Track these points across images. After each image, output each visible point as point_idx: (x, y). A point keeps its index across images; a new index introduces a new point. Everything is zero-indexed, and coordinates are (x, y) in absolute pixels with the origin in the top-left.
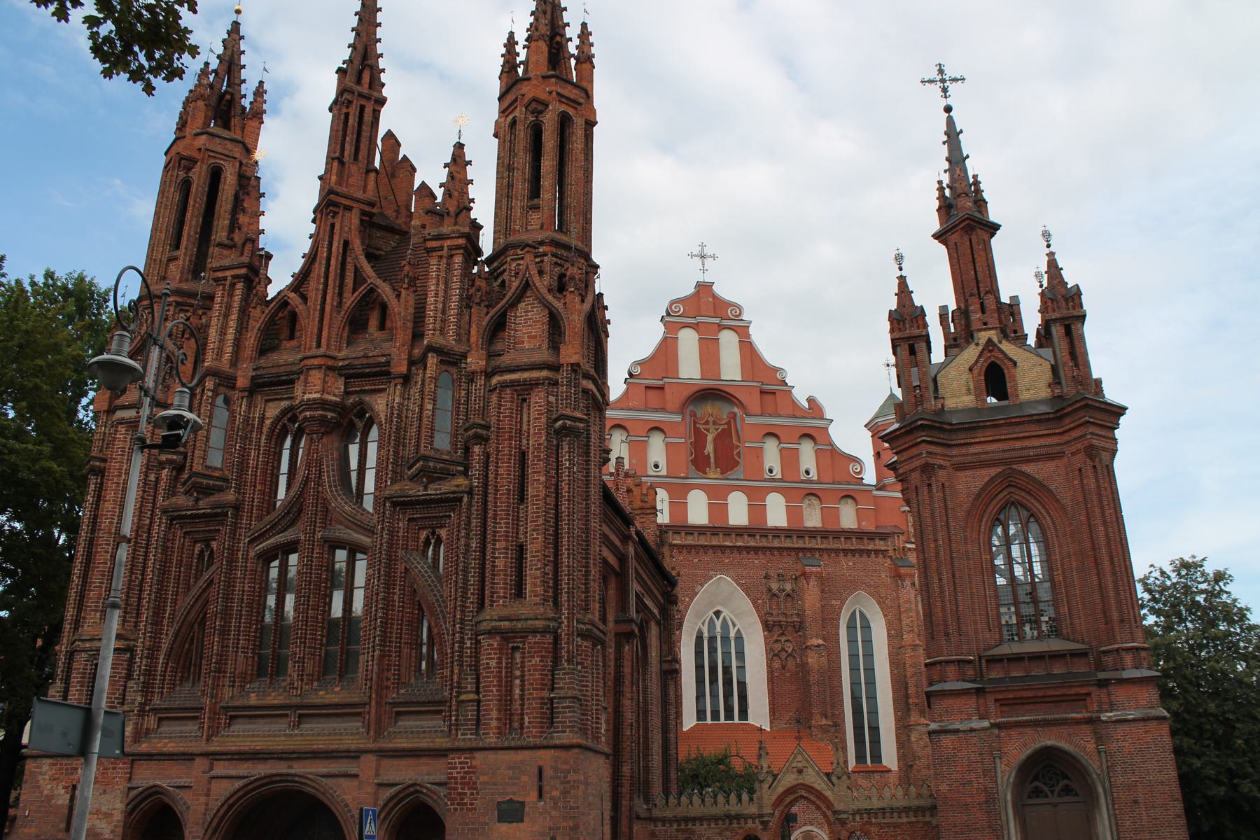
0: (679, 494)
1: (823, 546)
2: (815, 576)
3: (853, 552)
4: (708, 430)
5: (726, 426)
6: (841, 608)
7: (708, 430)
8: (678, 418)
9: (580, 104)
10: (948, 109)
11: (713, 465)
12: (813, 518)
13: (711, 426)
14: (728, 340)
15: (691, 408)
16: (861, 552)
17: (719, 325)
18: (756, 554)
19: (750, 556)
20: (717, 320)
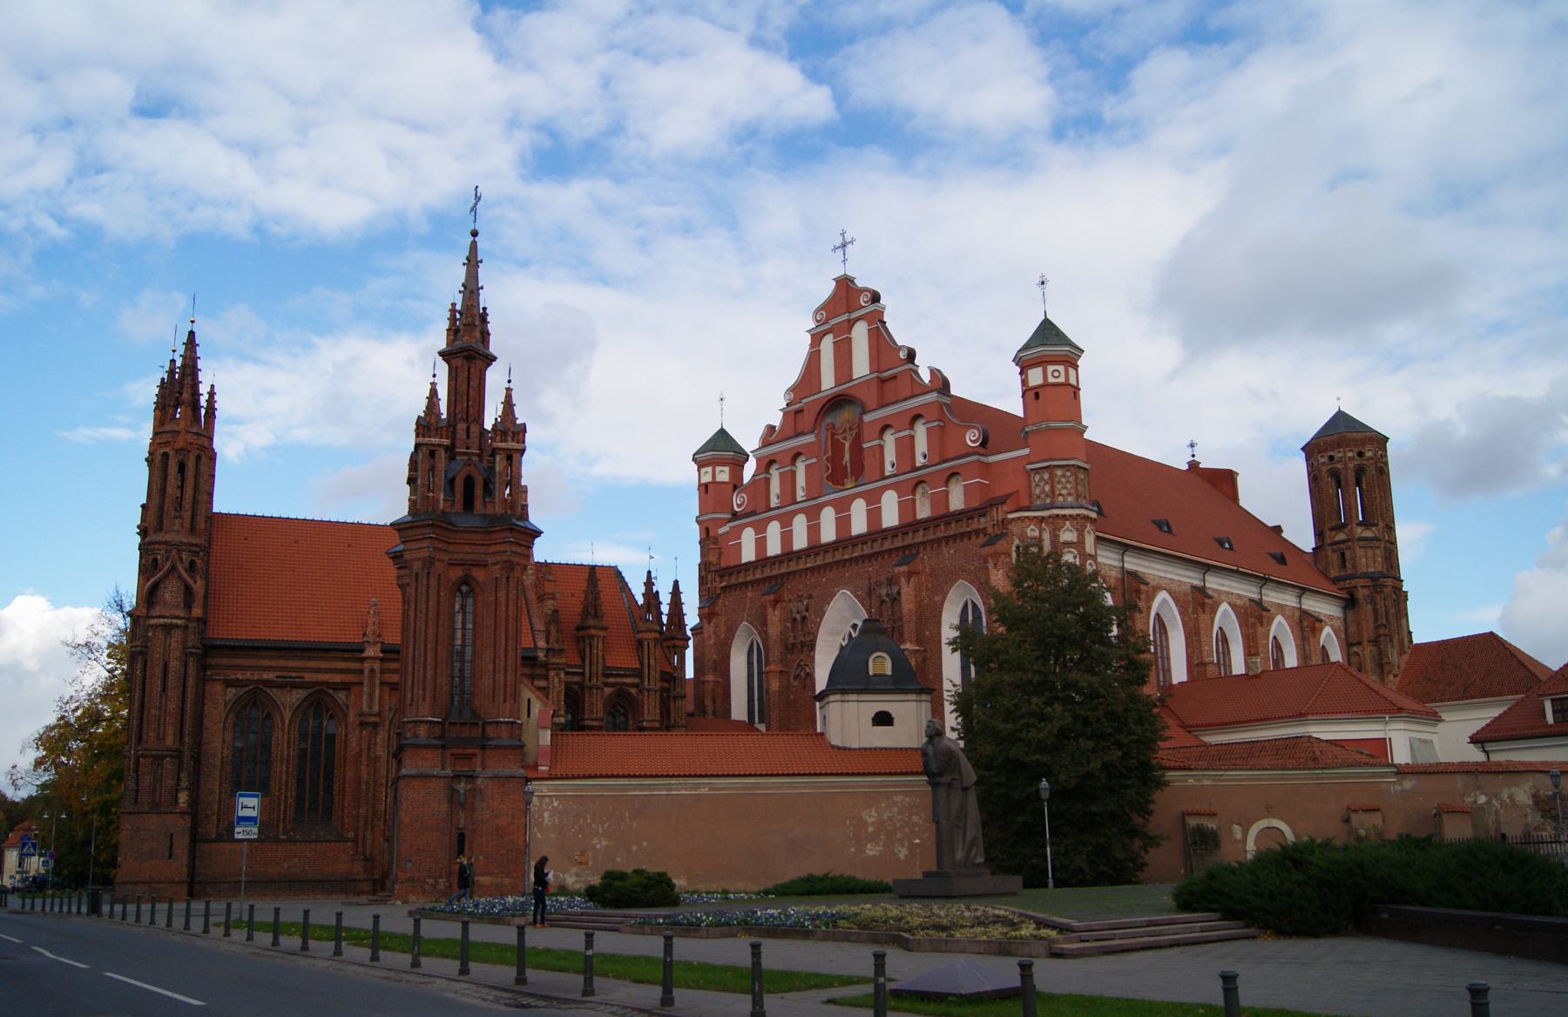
0: (813, 515)
1: (925, 539)
2: (904, 576)
3: (954, 538)
4: (845, 439)
5: (857, 430)
6: (942, 604)
7: (845, 439)
8: (810, 438)
9: (170, 442)
10: (475, 234)
11: (849, 474)
12: (923, 511)
13: (848, 435)
14: (860, 333)
15: (828, 420)
16: (962, 536)
17: (849, 320)
18: (870, 561)
19: (866, 565)
20: (845, 317)
